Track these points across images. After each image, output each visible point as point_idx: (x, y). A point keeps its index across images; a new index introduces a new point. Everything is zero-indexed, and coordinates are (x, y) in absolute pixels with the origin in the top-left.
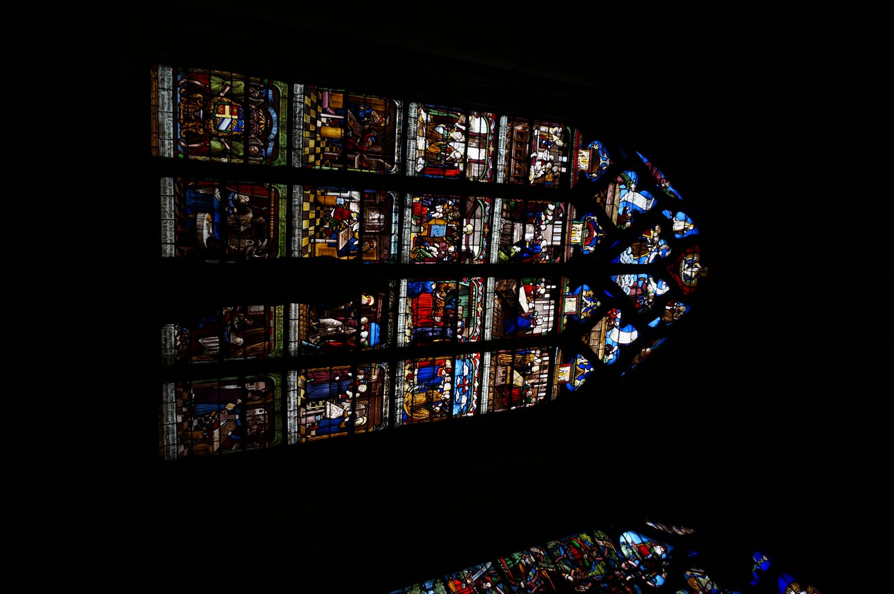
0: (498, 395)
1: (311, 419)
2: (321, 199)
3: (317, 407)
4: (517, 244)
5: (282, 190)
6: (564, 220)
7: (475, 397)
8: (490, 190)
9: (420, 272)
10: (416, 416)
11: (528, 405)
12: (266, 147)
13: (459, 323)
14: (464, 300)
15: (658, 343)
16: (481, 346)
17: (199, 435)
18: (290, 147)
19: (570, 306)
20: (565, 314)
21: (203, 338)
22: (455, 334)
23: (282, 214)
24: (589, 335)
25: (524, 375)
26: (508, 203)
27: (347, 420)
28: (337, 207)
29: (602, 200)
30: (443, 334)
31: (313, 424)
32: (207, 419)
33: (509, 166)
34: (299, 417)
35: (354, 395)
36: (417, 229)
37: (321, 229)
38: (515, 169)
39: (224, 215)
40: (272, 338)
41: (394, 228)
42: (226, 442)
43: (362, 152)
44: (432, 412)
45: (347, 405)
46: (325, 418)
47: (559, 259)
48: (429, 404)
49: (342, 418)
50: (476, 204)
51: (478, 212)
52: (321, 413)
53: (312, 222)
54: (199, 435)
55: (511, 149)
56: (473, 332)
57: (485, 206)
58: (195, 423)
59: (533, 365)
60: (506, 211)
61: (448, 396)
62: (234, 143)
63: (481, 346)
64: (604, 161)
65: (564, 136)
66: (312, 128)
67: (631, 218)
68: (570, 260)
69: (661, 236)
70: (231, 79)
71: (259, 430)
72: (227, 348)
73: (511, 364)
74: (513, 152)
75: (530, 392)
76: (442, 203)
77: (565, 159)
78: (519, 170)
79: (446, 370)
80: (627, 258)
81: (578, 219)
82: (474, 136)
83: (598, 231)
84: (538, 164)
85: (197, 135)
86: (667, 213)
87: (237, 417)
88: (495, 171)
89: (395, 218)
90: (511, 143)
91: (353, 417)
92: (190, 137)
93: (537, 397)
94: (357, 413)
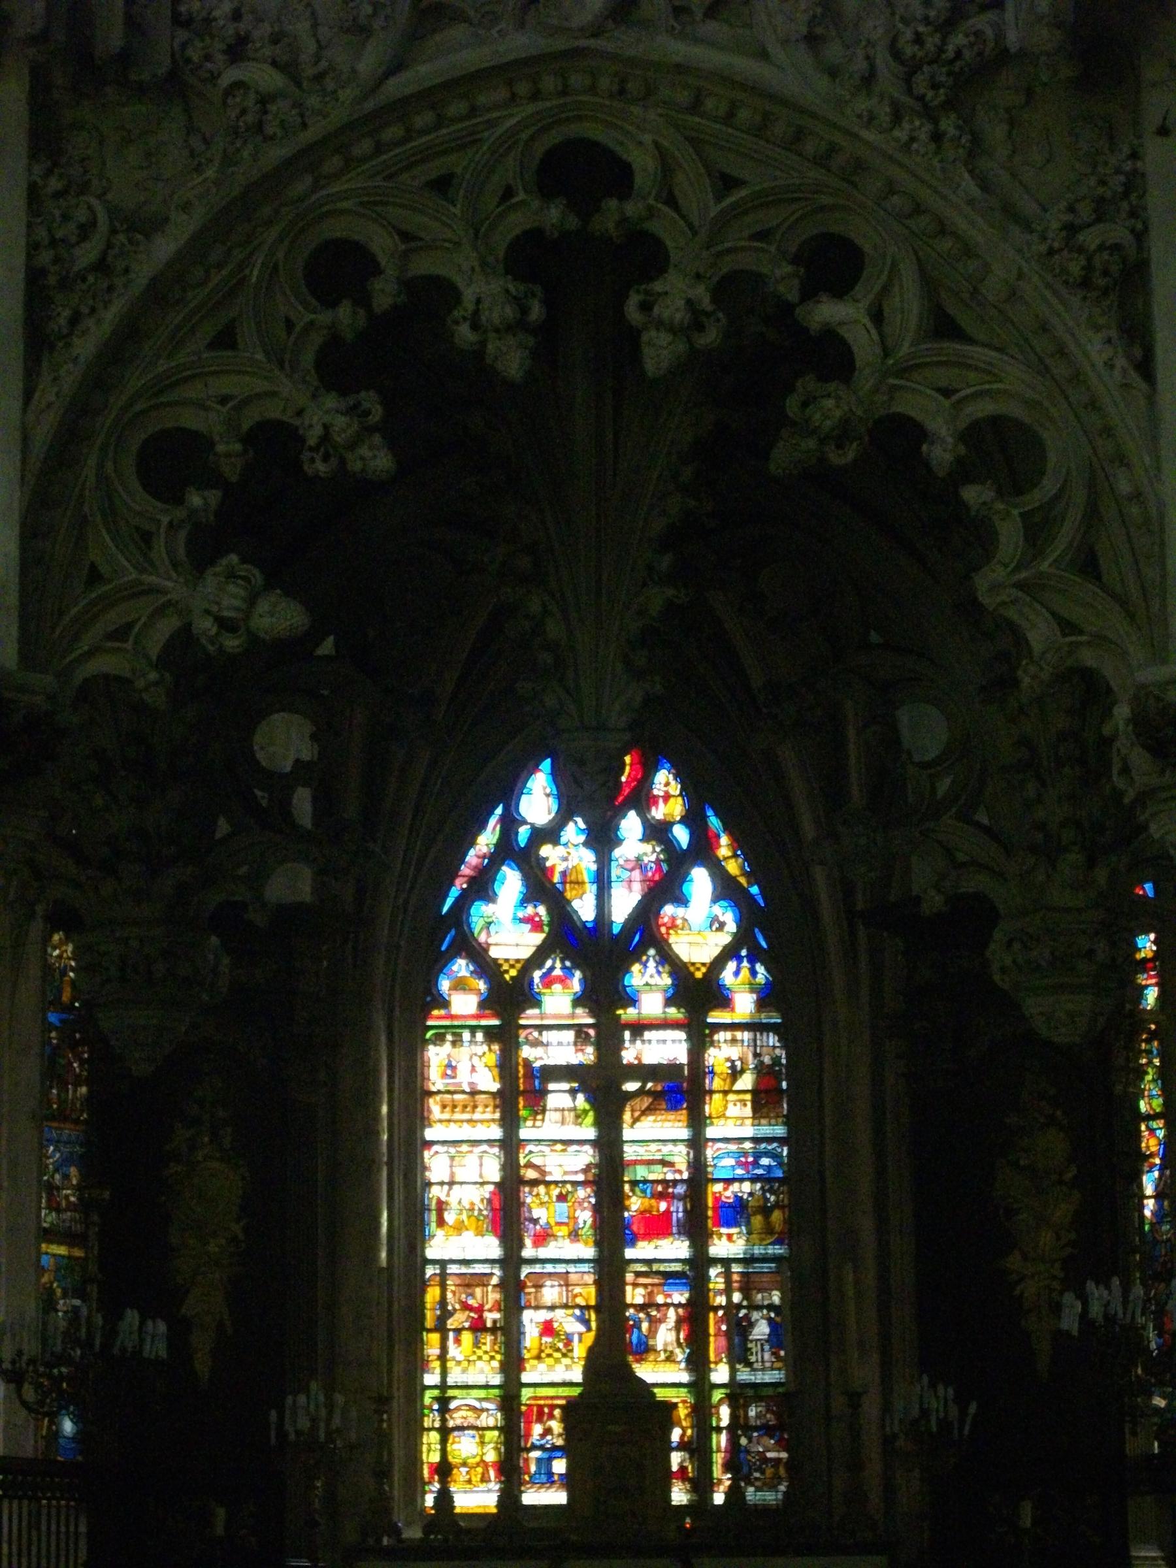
0: (765, 1110)
1: (767, 1356)
2: (535, 1352)
3: (754, 1351)
4: (574, 1099)
5: (526, 1394)
6: (541, 1028)
7: (763, 1145)
8: (510, 1145)
9: (612, 1231)
10: (778, 1228)
11: (784, 1061)
12: (488, 1410)
13: (670, 1177)
14: (641, 1172)
15: (714, 822)
16: (697, 1143)
17: (769, 1472)
18: (487, 1387)
19: (652, 1005)
20: (664, 1012)
21: (670, 1467)
22: (682, 1181)
23: (550, 1392)
24: (693, 964)
25: (742, 1071)
26: (525, 1119)
27: (772, 1315)
28: (542, 1335)
29: (512, 966)
30: (681, 1198)
31: (773, 1354)
32: (755, 1464)
33: (482, 1121)
34: (763, 1370)
35: (744, 1307)
36: (560, 1240)
37: (564, 1350)
38: (484, 1112)
39: (555, 1448)
40: (675, 1400)
41: (561, 1268)
42: (781, 1445)
43: (483, 1311)
44: (777, 1205)
45: (755, 1315)
46: (767, 1341)
47: (592, 1032)
48: (766, 1211)
49: (770, 1321)
50: (530, 1165)
51: (537, 1161)
52: (762, 1345)
53: (557, 1361)
54: (769, 1472)
55: (462, 1121)
56: (681, 1156)
57: (531, 1152)
58: (757, 1475)
59: (728, 1060)
60: (535, 1120)
61: (758, 1186)
62: (487, 1440)
63: (697, 1143)
64: (461, 967)
65: (439, 1039)
66: (465, 1364)
67: (535, 907)
68: (592, 1013)
69: (555, 841)
70: (429, 1444)
71: (773, 1412)
72: (682, 1446)
73: (725, 1093)
74: (466, 1116)
75: (767, 1060)
76: (530, 1211)
77: (466, 1035)
78: (486, 1106)
79: (725, 1189)
80: (585, 908)
81: (537, 1004)
82: (452, 1175)
83: (552, 968)
84: (475, 1078)
85: (483, 1474)
86: (523, 833)
87: (755, 1434)
88: (490, 1142)
89: (549, 1268)
90: (455, 1121)
91: (771, 1307)
92: (484, 1479)
93: (774, 1047)
94: (766, 1303)
